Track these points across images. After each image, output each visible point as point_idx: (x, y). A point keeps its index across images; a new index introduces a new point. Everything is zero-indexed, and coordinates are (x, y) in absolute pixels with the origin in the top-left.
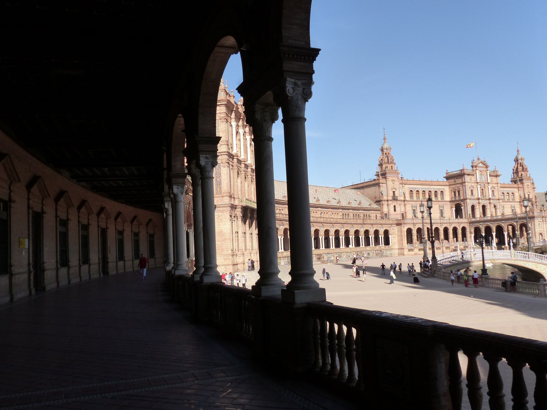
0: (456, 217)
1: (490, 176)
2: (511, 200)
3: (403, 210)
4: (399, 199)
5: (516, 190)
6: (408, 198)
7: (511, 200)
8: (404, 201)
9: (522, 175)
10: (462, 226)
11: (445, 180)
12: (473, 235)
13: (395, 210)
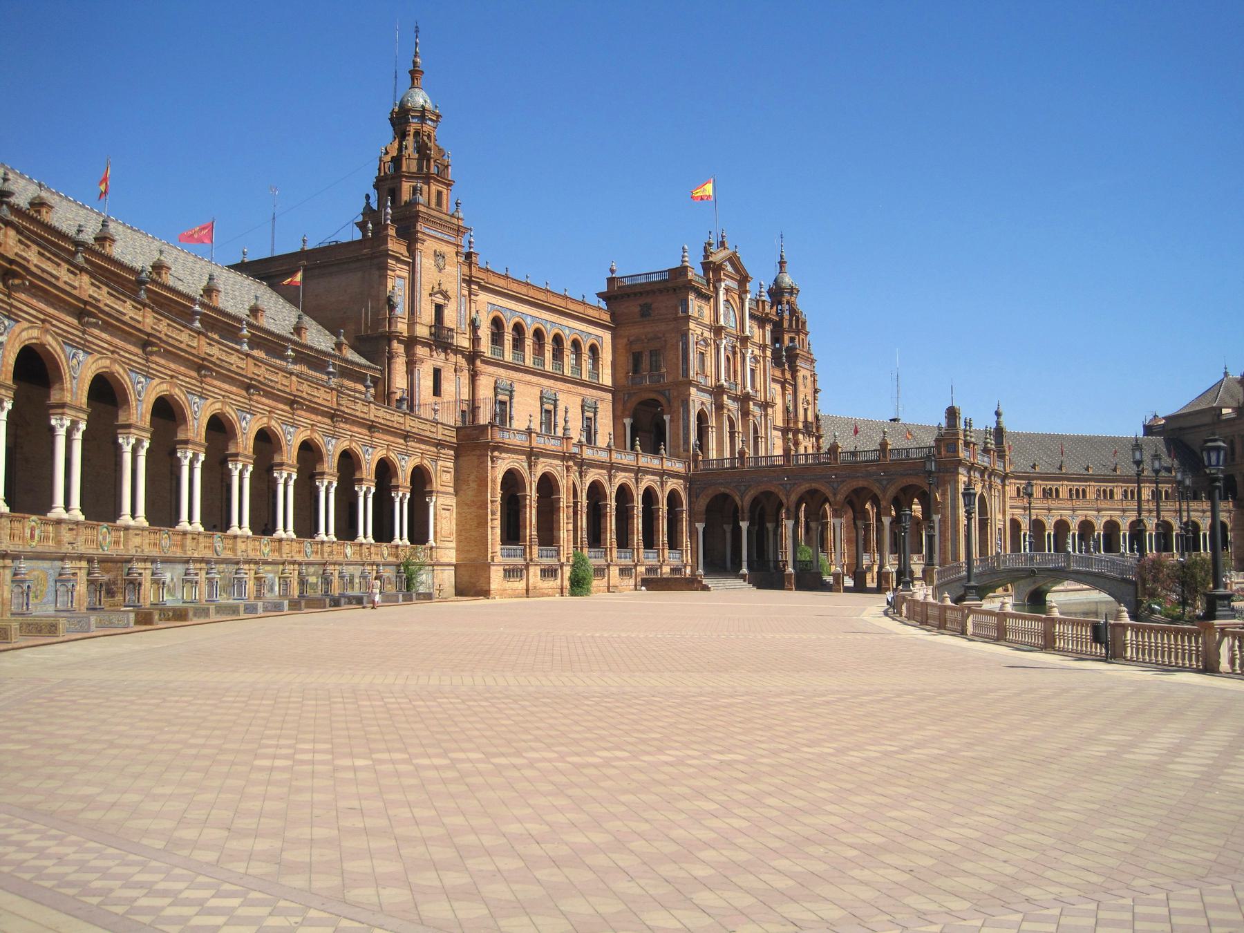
1: (752, 316)
5: (778, 387)
9: (792, 340)
10: (671, 484)
11: (603, 305)
12: (700, 526)
13: (437, 391)
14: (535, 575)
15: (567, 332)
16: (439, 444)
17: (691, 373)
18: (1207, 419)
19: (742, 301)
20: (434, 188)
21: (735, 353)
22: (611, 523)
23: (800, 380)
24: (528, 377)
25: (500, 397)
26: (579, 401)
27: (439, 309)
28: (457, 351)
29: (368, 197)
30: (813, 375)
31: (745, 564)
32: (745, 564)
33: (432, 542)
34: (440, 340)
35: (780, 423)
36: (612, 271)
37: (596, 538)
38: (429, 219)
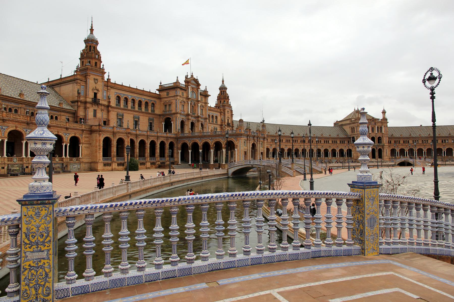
0: (165, 131)
2: (214, 123)
3: (105, 116)
4: (101, 102)
5: (219, 114)
6: (113, 103)
7: (214, 123)
8: (108, 106)
10: (170, 140)
11: (157, 92)
12: (180, 151)
13: (95, 115)
14: (115, 165)
15: (143, 100)
16: (83, 130)
17: (178, 110)
18: (348, 122)
19: (198, 91)
21: (195, 105)
22: (148, 151)
23: (226, 112)
24: (129, 112)
26: (147, 118)
27: (95, 94)
28: (102, 105)
30: (232, 111)
31: (190, 162)
32: (190, 162)
33: (80, 157)
35: (219, 123)
37: (142, 154)
38: (92, 69)
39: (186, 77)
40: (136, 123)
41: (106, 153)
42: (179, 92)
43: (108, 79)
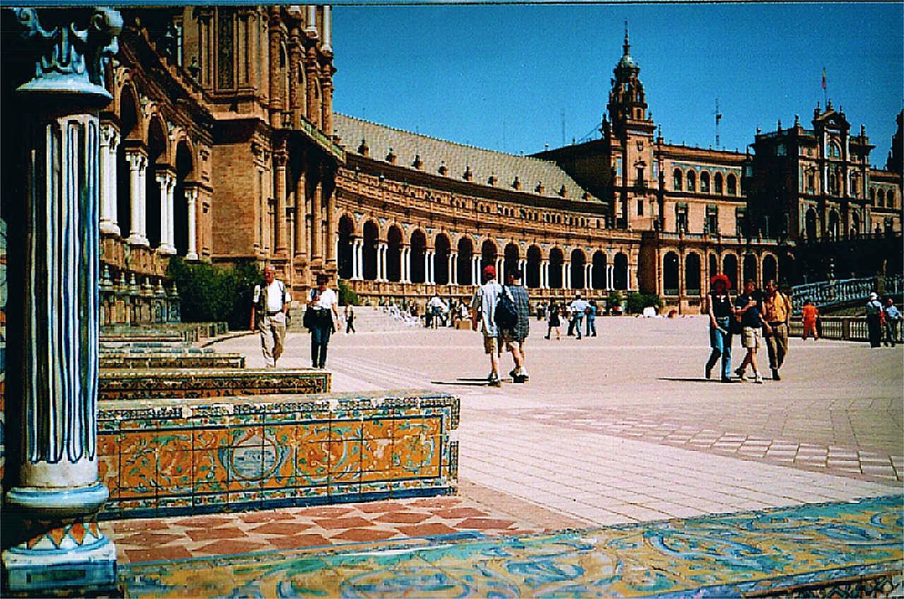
6: (669, 187)
13: (640, 212)
16: (631, 242)
17: (800, 188)
19: (844, 140)
20: (635, 109)
25: (680, 212)
26: (734, 208)
27: (641, 171)
28: (653, 191)
29: (605, 116)
34: (640, 188)
36: (758, 131)
39: (817, 115)
40: (712, 221)
41: (671, 283)
42: (803, 151)
43: (659, 139)
